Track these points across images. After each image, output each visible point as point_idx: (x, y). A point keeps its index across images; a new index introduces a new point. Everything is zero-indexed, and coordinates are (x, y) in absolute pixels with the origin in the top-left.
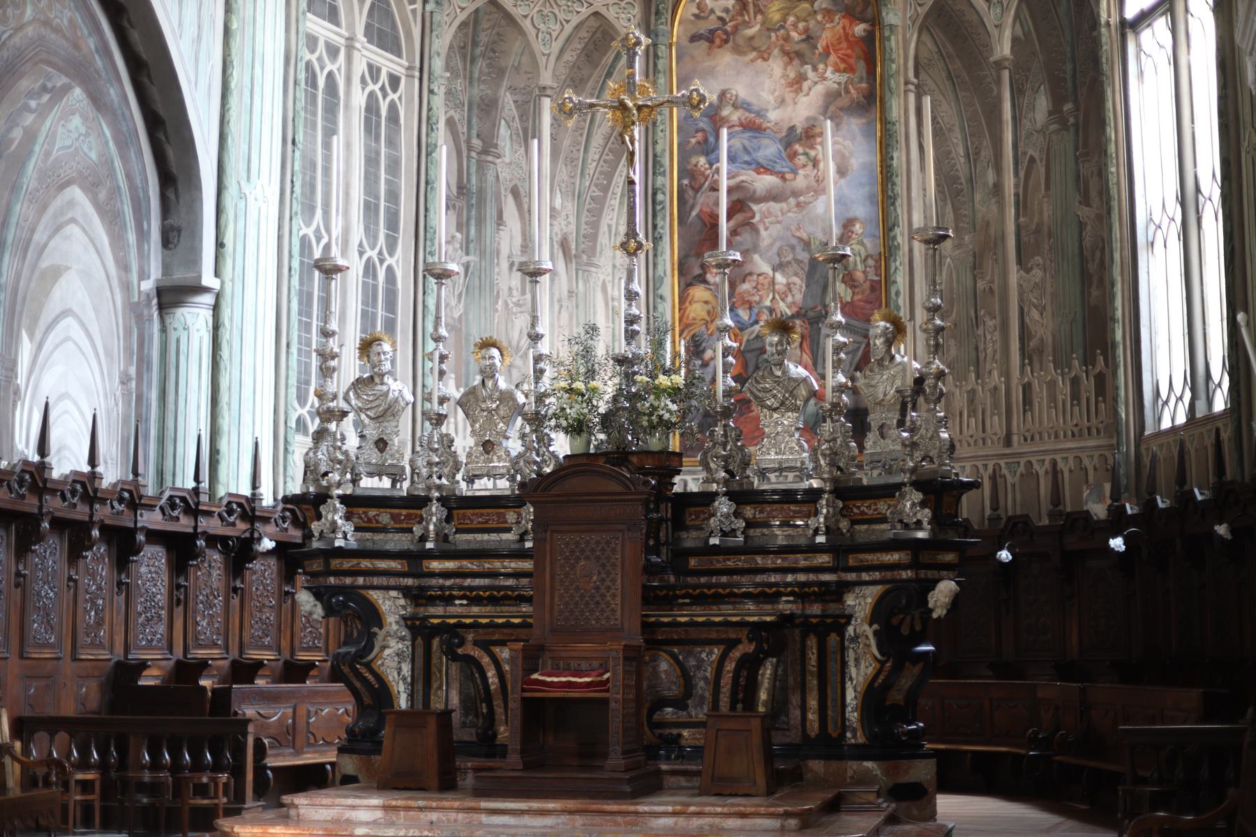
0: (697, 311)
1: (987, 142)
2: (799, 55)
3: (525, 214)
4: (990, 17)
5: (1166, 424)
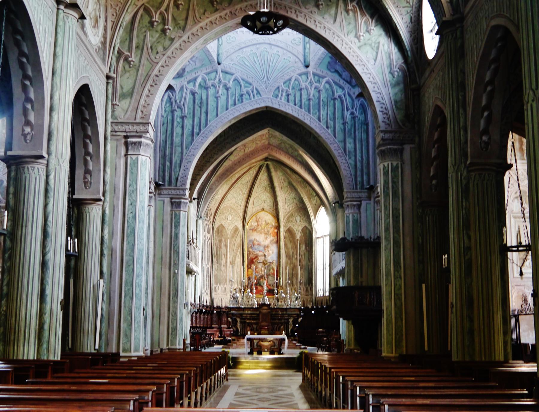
0: (250, 273)
1: (295, 251)
2: (267, 234)
3: (226, 258)
4: (297, 233)
5: (320, 296)
